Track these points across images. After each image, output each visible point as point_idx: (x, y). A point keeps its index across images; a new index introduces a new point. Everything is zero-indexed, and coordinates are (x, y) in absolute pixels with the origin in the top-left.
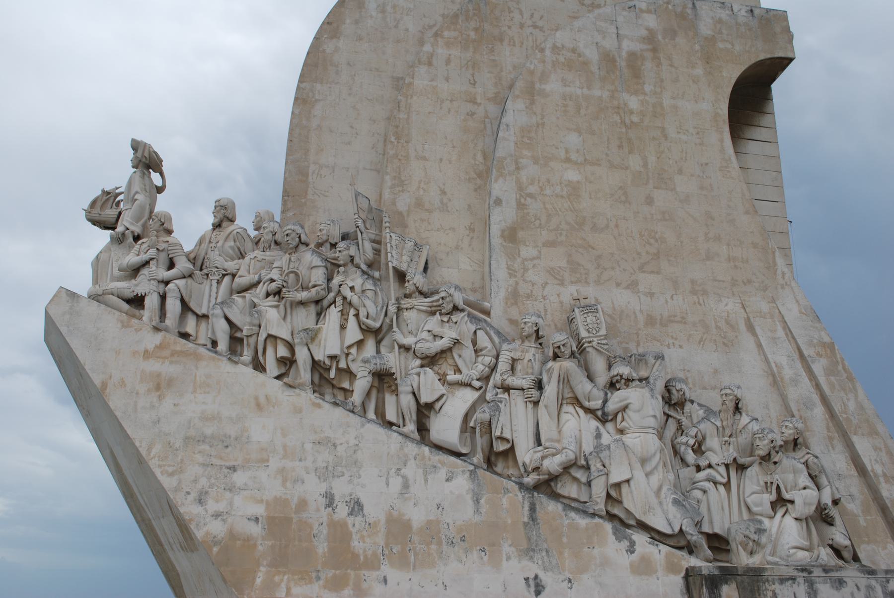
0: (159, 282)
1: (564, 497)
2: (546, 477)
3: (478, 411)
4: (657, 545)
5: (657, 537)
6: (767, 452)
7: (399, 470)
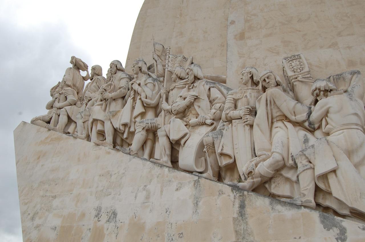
0: (58, 109)
1: (279, 196)
2: (259, 179)
7: (145, 186)
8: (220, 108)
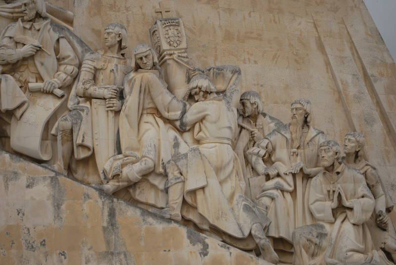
1: (142, 203)
2: (125, 184)
3: (59, 119)
4: (228, 248)
5: (228, 240)
6: (331, 163)
8: (72, 73)
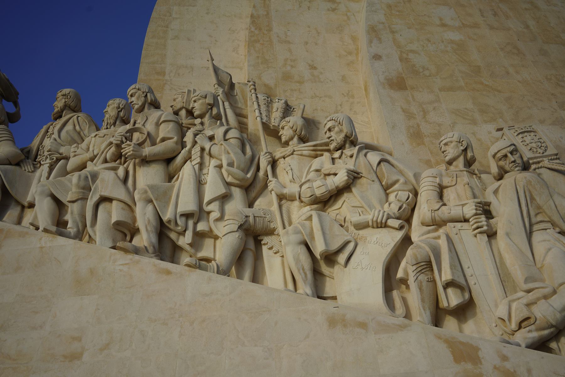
2: (546, 332)
